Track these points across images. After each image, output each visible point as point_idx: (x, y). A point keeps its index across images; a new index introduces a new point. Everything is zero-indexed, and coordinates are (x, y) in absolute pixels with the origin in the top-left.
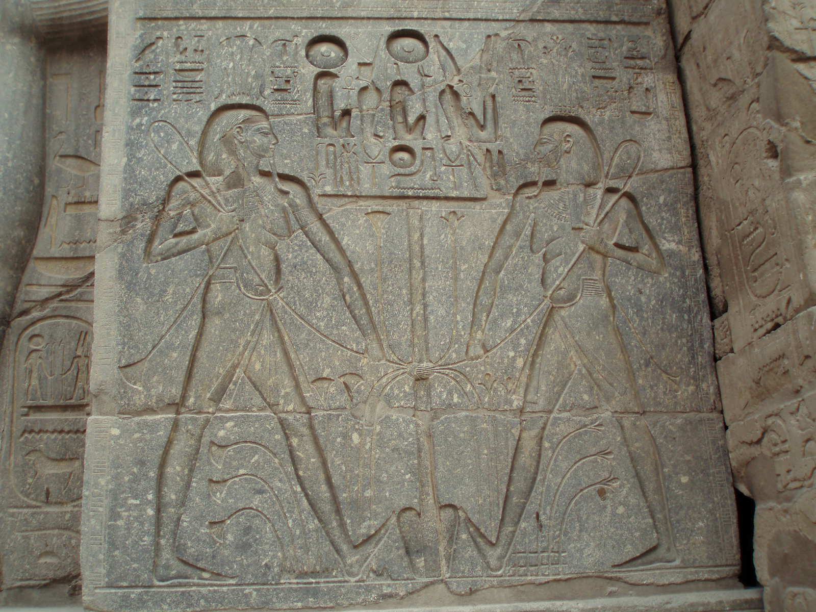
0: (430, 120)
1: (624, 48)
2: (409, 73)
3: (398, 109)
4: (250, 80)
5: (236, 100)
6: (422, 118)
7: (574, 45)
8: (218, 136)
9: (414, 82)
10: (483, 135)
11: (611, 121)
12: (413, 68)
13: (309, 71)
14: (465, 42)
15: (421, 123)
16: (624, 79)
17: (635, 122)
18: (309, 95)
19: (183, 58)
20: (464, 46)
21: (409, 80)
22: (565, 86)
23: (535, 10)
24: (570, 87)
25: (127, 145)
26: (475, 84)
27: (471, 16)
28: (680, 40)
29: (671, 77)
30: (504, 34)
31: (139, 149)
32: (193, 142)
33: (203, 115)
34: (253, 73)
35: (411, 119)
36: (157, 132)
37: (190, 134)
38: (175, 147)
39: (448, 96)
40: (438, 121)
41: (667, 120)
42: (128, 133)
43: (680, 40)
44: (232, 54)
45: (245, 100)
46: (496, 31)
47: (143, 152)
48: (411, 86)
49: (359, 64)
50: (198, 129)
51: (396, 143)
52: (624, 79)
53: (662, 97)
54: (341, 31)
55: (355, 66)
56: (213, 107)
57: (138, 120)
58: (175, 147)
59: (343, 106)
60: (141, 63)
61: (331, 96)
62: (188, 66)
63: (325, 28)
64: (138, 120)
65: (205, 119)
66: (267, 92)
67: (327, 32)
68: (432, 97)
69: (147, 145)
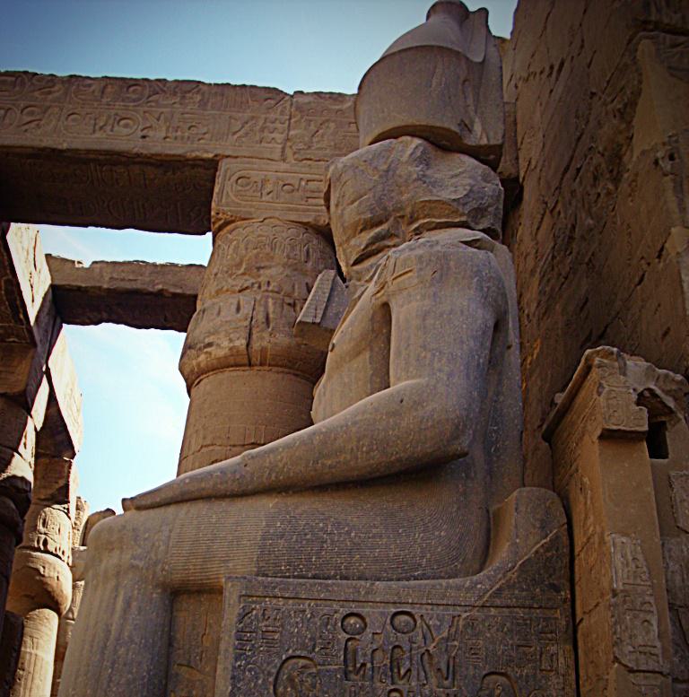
0: (414, 673)
1: (540, 626)
2: (403, 640)
3: (394, 664)
4: (307, 641)
5: (298, 653)
6: (409, 670)
7: (508, 624)
8: (285, 677)
9: (406, 647)
10: (446, 683)
11: (527, 676)
12: (406, 637)
13: (343, 636)
14: (440, 621)
15: (408, 674)
16: (538, 649)
17: (543, 677)
18: (342, 652)
19: (267, 623)
20: (438, 623)
21: (403, 645)
22: (499, 653)
23: (485, 599)
24: (503, 653)
25: (232, 678)
26: (443, 650)
27: (445, 602)
28: (577, 621)
29: (569, 647)
30: (464, 615)
31: (239, 682)
32: (271, 679)
33: (277, 662)
34: (309, 636)
35: (402, 672)
36: (250, 671)
37: (269, 674)
38: (260, 682)
39: (426, 657)
40: (418, 675)
41: (563, 676)
42: (232, 671)
43: (577, 621)
44: (297, 623)
45: (304, 653)
46: (459, 613)
47: (242, 683)
48: (404, 649)
49: (373, 633)
50: (274, 671)
51: (392, 687)
52: (538, 649)
53: (561, 660)
54: (364, 611)
55: (370, 635)
56: (284, 657)
57: (239, 663)
58: (260, 682)
59: (362, 661)
60: (242, 625)
61: (355, 652)
62: (270, 628)
63: (354, 608)
64: (239, 663)
65: (278, 665)
66: (317, 649)
67: (355, 611)
68: (416, 658)
69: (244, 679)
